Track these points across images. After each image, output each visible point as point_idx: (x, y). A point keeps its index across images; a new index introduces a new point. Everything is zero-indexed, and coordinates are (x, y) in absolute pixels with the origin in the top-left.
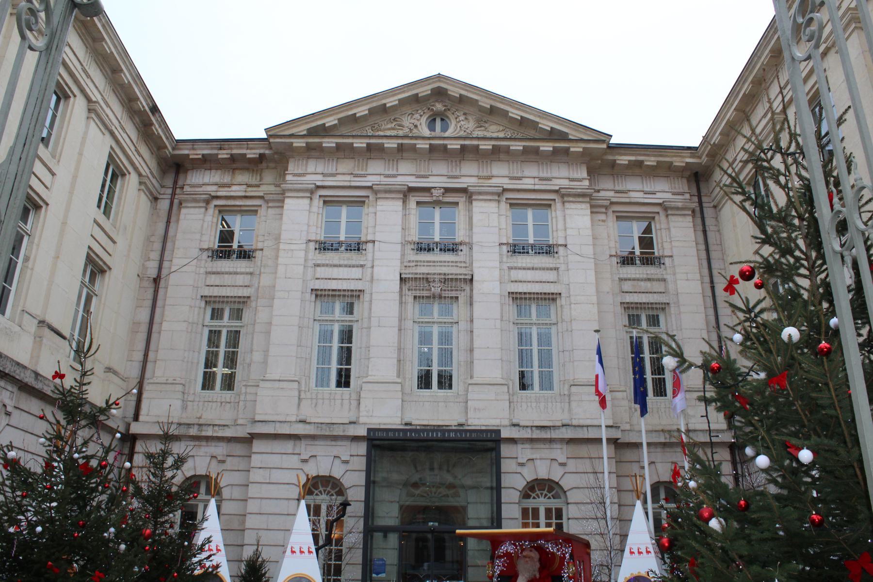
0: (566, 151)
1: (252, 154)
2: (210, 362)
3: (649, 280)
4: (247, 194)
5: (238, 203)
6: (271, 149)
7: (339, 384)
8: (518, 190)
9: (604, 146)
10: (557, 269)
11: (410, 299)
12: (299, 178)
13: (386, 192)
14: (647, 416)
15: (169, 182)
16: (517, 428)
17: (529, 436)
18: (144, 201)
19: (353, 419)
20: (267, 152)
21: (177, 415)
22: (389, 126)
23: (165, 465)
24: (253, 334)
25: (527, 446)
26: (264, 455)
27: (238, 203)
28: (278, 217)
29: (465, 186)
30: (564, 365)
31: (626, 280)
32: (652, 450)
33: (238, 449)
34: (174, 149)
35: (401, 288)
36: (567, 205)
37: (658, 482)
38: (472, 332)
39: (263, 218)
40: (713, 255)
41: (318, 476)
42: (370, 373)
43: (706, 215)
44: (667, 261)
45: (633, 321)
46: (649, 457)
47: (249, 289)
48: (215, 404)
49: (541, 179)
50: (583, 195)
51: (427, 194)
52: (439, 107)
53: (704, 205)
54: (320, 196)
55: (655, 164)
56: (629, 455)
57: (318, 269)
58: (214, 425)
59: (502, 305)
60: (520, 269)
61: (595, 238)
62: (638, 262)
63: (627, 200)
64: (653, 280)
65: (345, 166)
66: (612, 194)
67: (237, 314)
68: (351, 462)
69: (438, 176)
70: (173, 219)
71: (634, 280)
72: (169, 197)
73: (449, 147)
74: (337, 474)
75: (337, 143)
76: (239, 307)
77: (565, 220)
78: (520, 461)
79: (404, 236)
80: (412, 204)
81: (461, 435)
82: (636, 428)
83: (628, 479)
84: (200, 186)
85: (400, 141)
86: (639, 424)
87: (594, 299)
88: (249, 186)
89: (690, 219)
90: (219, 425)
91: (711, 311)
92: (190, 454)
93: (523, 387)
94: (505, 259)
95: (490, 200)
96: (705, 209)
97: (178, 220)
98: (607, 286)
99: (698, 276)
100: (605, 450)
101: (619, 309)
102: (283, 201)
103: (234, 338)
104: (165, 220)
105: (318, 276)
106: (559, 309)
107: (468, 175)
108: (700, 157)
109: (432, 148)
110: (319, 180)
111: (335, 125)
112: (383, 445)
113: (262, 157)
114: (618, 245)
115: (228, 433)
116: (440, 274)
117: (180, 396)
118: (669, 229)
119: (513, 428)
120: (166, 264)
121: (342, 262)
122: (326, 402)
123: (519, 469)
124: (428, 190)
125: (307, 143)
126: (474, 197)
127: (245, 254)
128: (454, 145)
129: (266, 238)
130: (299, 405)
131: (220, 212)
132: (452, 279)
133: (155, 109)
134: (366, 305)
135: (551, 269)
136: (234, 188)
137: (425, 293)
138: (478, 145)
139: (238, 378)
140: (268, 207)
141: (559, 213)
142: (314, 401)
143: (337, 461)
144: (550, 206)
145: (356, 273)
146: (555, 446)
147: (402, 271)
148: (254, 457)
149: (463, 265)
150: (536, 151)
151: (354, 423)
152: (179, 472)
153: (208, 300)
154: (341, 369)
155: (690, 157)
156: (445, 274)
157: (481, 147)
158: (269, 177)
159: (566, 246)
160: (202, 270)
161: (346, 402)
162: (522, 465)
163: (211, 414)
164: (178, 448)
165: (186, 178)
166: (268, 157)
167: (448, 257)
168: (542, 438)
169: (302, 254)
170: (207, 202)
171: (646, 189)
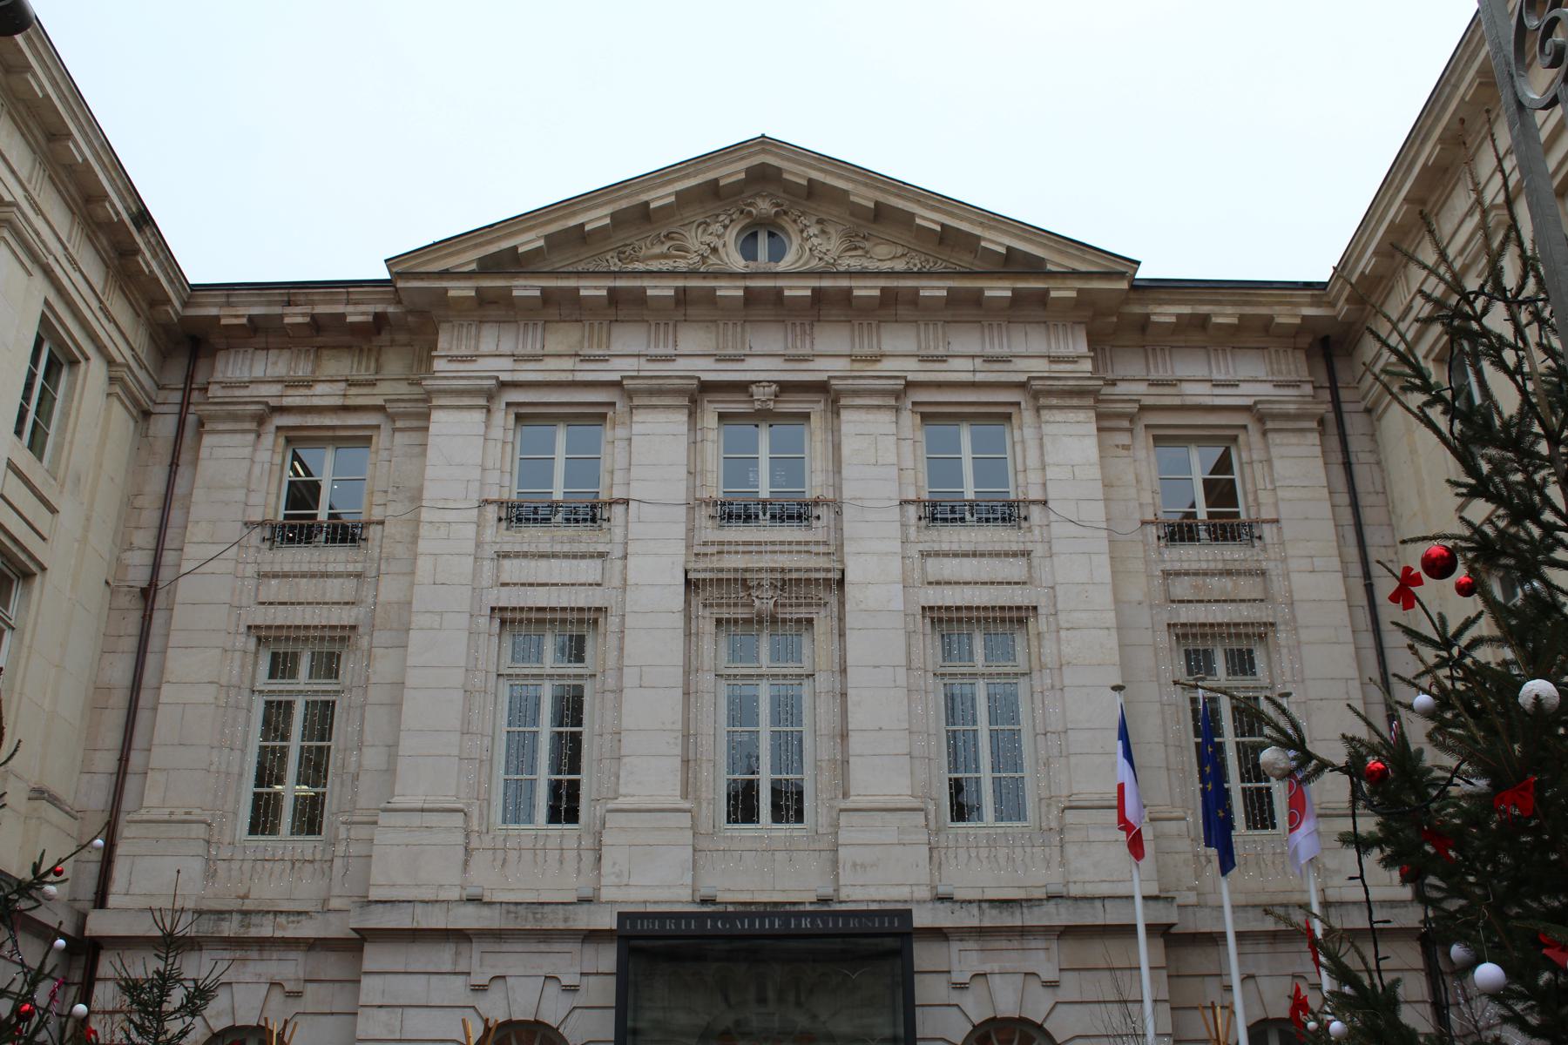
0: (1042, 298)
1: (357, 314)
2: (268, 772)
3: (1229, 573)
4: (349, 402)
5: (328, 420)
6: (399, 302)
7: (554, 816)
8: (940, 385)
9: (1124, 285)
10: (1026, 554)
11: (708, 627)
12: (461, 366)
13: (651, 392)
14: (1234, 872)
15: (176, 376)
16: (948, 904)
17: (975, 923)
18: (120, 417)
19: (587, 893)
20: (391, 309)
21: (194, 891)
22: (657, 250)
23: (165, 1007)
24: (363, 707)
25: (971, 945)
26: (388, 977)
27: (328, 420)
28: (418, 450)
29: (823, 377)
30: (1047, 764)
31: (1178, 574)
32: (1248, 948)
33: (331, 965)
34: (185, 305)
35: (687, 602)
36: (1046, 415)
37: (1265, 1021)
38: (844, 695)
39: (384, 454)
40: (1368, 515)
41: (509, 1024)
42: (622, 790)
43: (1349, 429)
44: (1268, 531)
45: (1198, 662)
46: (1241, 964)
47: (354, 611)
48: (278, 866)
49: (989, 359)
50: (1080, 393)
51: (743, 397)
52: (764, 207)
53: (1345, 407)
54: (508, 404)
55: (1234, 321)
56: (1197, 960)
57: (506, 563)
58: (276, 913)
60: (946, 555)
61: (1107, 485)
62: (1203, 535)
63: (1177, 401)
64: (1239, 573)
65: (563, 338)
66: (1141, 388)
67: (328, 666)
68: (582, 989)
69: (765, 358)
70: (185, 457)
71: (1196, 574)
72: (176, 409)
73: (787, 293)
74: (551, 1017)
75: (543, 289)
76: (333, 649)
77: (1041, 446)
78: (957, 977)
79: (691, 489)
80: (709, 420)
81: (825, 923)
82: (1211, 900)
83: (1197, 1014)
84: (244, 385)
85: (680, 283)
86: (1217, 891)
87: (1110, 618)
88: (351, 383)
89: (1314, 438)
90: (288, 913)
91: (1368, 640)
92: (224, 979)
93: (960, 811)
95: (879, 407)
96: (1346, 417)
98: (1136, 589)
99: (1336, 563)
100: (1144, 951)
101: (1164, 639)
102: (427, 416)
103: (322, 717)
105: (505, 578)
106: (1034, 643)
107: (830, 354)
108: (1332, 305)
109: (751, 297)
110: (504, 368)
111: (538, 250)
112: (656, 951)
113: (380, 318)
114: (1158, 500)
115: (308, 930)
116: (772, 570)
117: (200, 848)
118: (1269, 461)
119: (939, 905)
120: (168, 557)
121: (557, 548)
122: (527, 855)
123: (955, 997)
124: (742, 387)
125: (478, 289)
126: (843, 402)
127: (344, 534)
128: (799, 289)
129: (390, 496)
130: (466, 862)
131: (289, 440)
132: (798, 581)
133: (143, 218)
134: (612, 641)
135: (1015, 555)
136: (319, 388)
137: (741, 613)
138: (850, 289)
139: (330, 805)
140: (394, 430)
141: (1029, 433)
142: (500, 855)
143: (552, 988)
144: (1008, 417)
145: (588, 570)
146: (1033, 944)
147: (691, 565)
148: (366, 982)
149: (822, 549)
150: (976, 300)
151: (589, 901)
152: (198, 1019)
153: (262, 635)
154: (559, 782)
155: (1312, 305)
156: (783, 570)
157: (856, 293)
158: (394, 364)
159: (1045, 503)
160: (250, 570)
161: (570, 856)
162: (961, 987)
163: (270, 889)
164: (195, 967)
165: (213, 368)
166: (395, 321)
167: (790, 533)
168: (1003, 926)
169: (471, 531)
170: (261, 420)
171: (1216, 376)
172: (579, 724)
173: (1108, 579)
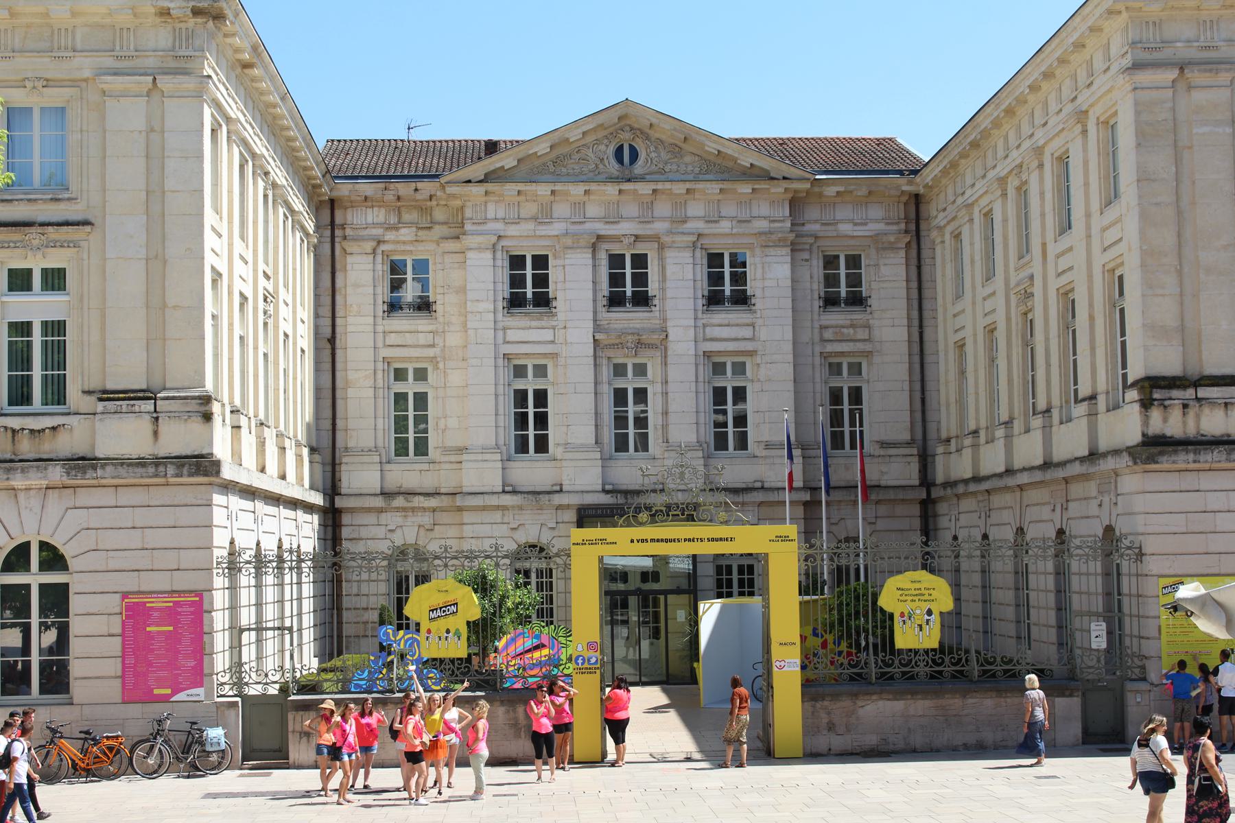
3: (852, 326)
45: (835, 369)
59: (697, 365)
87: (790, 358)
91: (917, 359)
94: (700, 315)
97: (345, 270)
99: (905, 322)
104: (329, 269)
114: (822, 285)
118: (877, 265)
120: (339, 321)
136: (403, 231)
145: (547, 335)
172: (546, 406)
173: (790, 337)
